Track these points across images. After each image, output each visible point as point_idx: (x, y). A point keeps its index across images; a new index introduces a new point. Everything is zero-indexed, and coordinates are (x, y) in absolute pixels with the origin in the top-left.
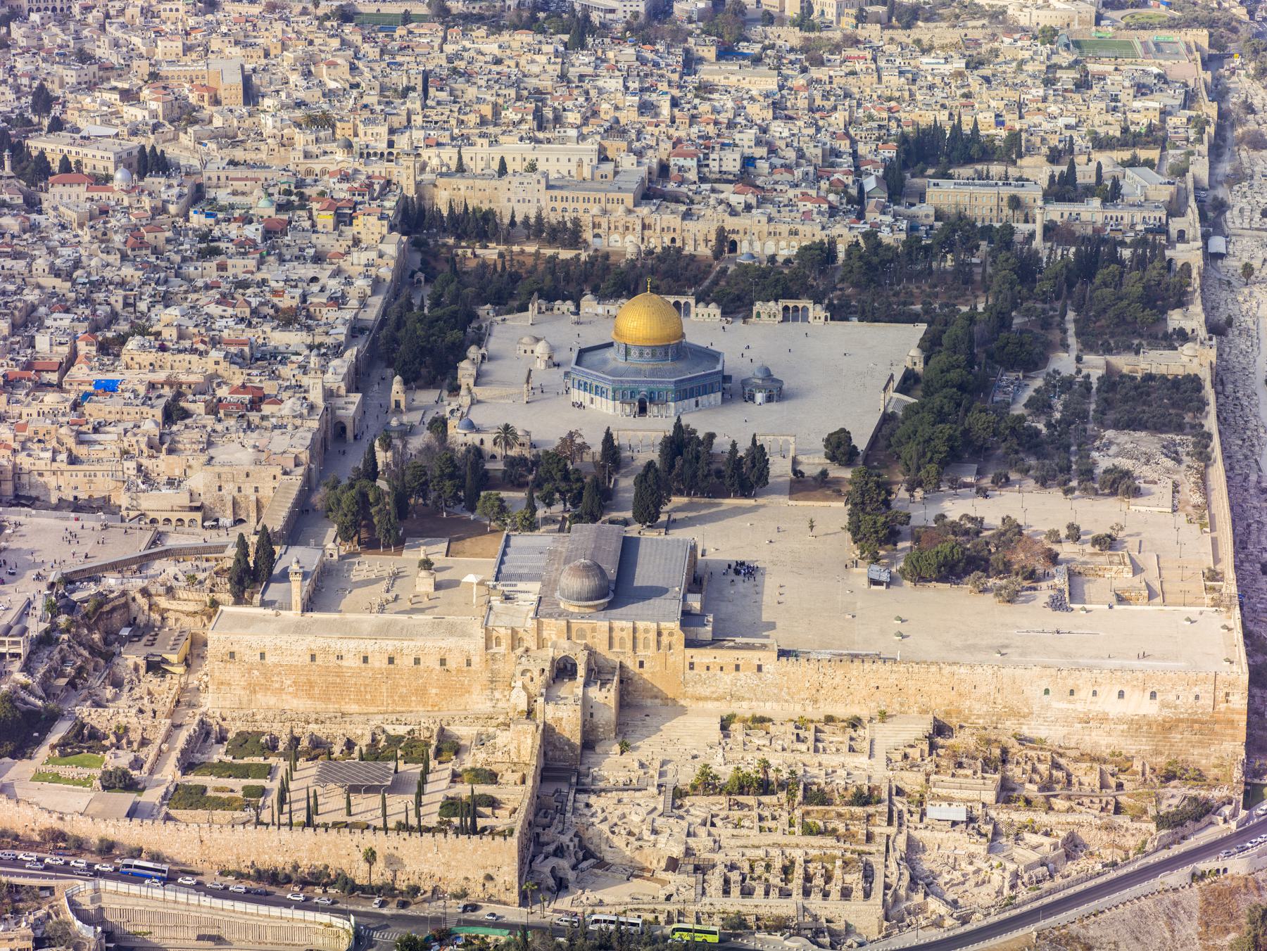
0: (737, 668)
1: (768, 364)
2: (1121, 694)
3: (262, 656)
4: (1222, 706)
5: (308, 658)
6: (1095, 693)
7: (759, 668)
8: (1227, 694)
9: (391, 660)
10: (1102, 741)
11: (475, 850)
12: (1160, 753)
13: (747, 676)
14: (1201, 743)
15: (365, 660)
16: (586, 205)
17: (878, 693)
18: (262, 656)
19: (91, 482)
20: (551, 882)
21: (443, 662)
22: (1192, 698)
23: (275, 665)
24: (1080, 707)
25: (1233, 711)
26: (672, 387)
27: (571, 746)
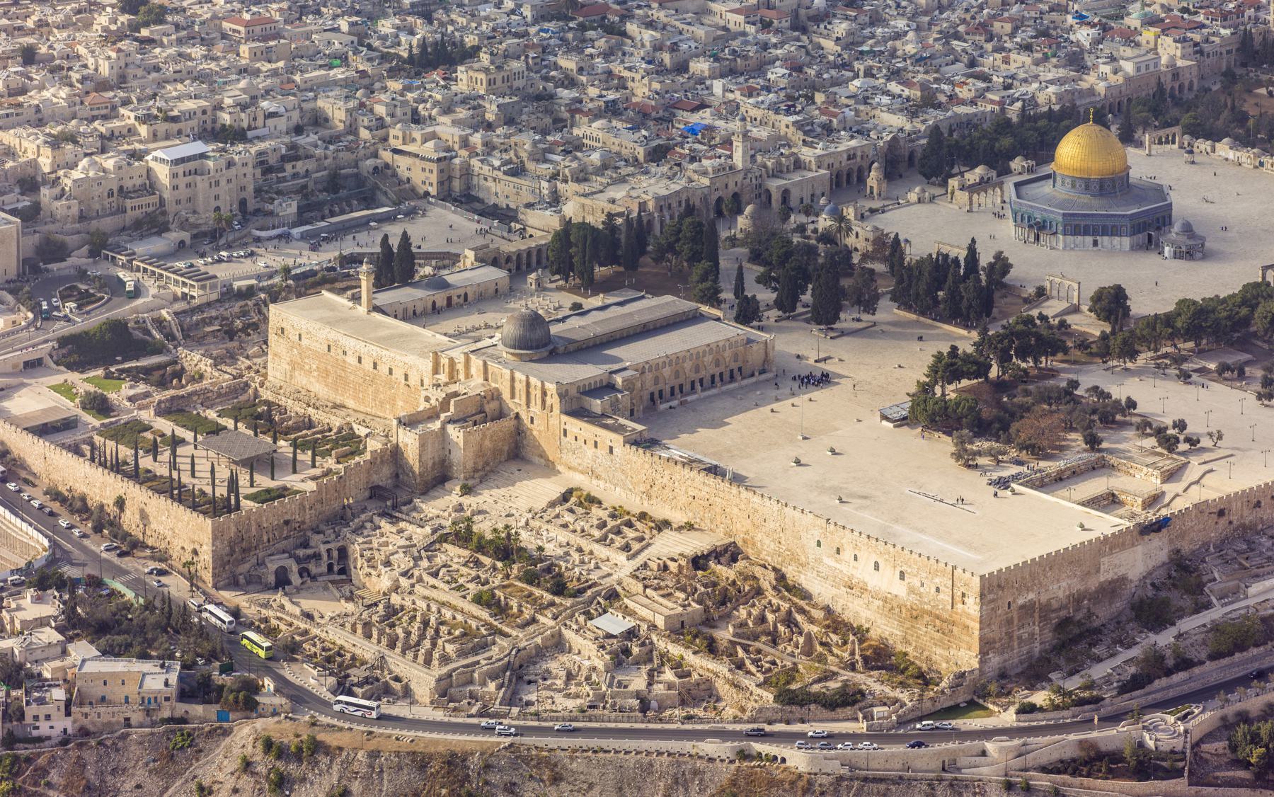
1: (1191, 220)
4: (959, 606)
6: (856, 558)
10: (857, 611)
19: (518, 194)
20: (272, 579)
25: (968, 616)
26: (1060, 219)
27: (413, 473)
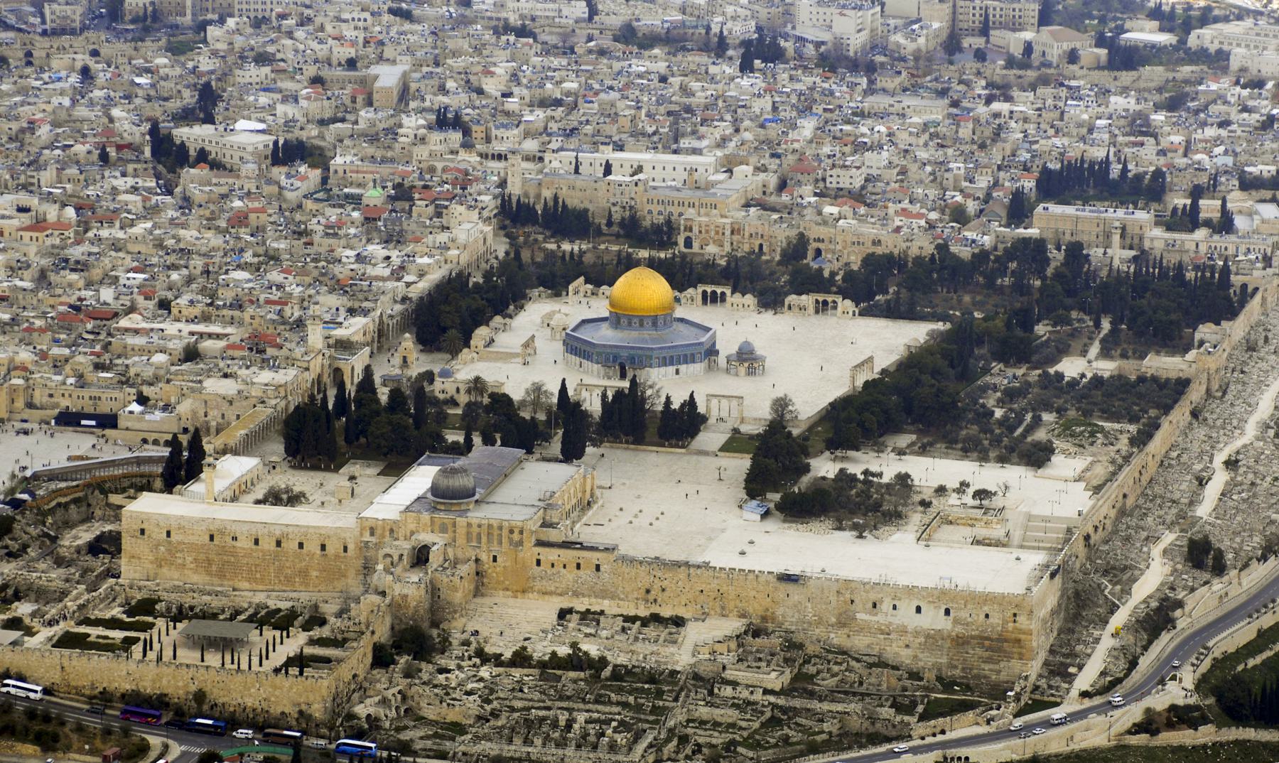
0: (578, 566)
2: (919, 610)
5: (208, 538)
6: (895, 607)
7: (598, 568)
8: (1015, 615)
9: (279, 544)
11: (291, 688)
12: (956, 667)
13: (586, 574)
14: (989, 660)
15: (256, 542)
16: (681, 209)
17: (702, 597)
21: (323, 547)
22: (982, 616)
23: (179, 543)
24: (880, 618)
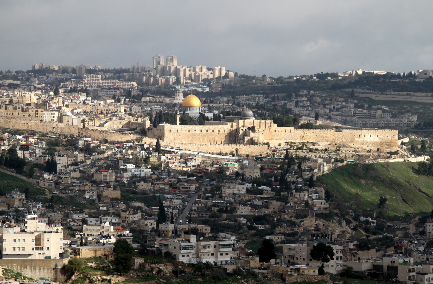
0: (285, 131)
2: (370, 136)
3: (177, 131)
9: (207, 131)
15: (201, 131)
18: (177, 131)
